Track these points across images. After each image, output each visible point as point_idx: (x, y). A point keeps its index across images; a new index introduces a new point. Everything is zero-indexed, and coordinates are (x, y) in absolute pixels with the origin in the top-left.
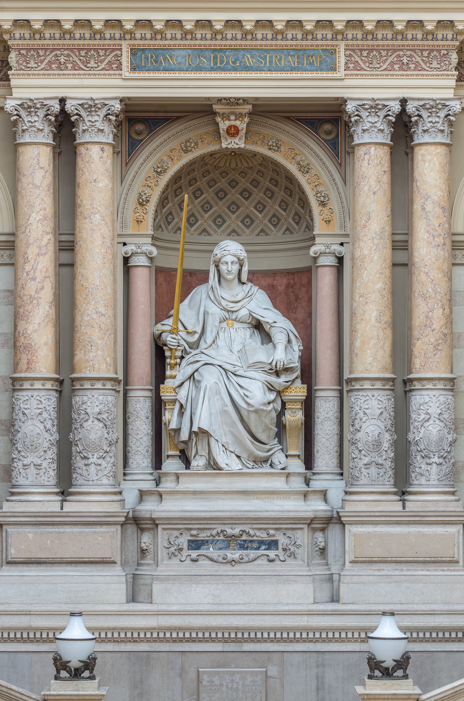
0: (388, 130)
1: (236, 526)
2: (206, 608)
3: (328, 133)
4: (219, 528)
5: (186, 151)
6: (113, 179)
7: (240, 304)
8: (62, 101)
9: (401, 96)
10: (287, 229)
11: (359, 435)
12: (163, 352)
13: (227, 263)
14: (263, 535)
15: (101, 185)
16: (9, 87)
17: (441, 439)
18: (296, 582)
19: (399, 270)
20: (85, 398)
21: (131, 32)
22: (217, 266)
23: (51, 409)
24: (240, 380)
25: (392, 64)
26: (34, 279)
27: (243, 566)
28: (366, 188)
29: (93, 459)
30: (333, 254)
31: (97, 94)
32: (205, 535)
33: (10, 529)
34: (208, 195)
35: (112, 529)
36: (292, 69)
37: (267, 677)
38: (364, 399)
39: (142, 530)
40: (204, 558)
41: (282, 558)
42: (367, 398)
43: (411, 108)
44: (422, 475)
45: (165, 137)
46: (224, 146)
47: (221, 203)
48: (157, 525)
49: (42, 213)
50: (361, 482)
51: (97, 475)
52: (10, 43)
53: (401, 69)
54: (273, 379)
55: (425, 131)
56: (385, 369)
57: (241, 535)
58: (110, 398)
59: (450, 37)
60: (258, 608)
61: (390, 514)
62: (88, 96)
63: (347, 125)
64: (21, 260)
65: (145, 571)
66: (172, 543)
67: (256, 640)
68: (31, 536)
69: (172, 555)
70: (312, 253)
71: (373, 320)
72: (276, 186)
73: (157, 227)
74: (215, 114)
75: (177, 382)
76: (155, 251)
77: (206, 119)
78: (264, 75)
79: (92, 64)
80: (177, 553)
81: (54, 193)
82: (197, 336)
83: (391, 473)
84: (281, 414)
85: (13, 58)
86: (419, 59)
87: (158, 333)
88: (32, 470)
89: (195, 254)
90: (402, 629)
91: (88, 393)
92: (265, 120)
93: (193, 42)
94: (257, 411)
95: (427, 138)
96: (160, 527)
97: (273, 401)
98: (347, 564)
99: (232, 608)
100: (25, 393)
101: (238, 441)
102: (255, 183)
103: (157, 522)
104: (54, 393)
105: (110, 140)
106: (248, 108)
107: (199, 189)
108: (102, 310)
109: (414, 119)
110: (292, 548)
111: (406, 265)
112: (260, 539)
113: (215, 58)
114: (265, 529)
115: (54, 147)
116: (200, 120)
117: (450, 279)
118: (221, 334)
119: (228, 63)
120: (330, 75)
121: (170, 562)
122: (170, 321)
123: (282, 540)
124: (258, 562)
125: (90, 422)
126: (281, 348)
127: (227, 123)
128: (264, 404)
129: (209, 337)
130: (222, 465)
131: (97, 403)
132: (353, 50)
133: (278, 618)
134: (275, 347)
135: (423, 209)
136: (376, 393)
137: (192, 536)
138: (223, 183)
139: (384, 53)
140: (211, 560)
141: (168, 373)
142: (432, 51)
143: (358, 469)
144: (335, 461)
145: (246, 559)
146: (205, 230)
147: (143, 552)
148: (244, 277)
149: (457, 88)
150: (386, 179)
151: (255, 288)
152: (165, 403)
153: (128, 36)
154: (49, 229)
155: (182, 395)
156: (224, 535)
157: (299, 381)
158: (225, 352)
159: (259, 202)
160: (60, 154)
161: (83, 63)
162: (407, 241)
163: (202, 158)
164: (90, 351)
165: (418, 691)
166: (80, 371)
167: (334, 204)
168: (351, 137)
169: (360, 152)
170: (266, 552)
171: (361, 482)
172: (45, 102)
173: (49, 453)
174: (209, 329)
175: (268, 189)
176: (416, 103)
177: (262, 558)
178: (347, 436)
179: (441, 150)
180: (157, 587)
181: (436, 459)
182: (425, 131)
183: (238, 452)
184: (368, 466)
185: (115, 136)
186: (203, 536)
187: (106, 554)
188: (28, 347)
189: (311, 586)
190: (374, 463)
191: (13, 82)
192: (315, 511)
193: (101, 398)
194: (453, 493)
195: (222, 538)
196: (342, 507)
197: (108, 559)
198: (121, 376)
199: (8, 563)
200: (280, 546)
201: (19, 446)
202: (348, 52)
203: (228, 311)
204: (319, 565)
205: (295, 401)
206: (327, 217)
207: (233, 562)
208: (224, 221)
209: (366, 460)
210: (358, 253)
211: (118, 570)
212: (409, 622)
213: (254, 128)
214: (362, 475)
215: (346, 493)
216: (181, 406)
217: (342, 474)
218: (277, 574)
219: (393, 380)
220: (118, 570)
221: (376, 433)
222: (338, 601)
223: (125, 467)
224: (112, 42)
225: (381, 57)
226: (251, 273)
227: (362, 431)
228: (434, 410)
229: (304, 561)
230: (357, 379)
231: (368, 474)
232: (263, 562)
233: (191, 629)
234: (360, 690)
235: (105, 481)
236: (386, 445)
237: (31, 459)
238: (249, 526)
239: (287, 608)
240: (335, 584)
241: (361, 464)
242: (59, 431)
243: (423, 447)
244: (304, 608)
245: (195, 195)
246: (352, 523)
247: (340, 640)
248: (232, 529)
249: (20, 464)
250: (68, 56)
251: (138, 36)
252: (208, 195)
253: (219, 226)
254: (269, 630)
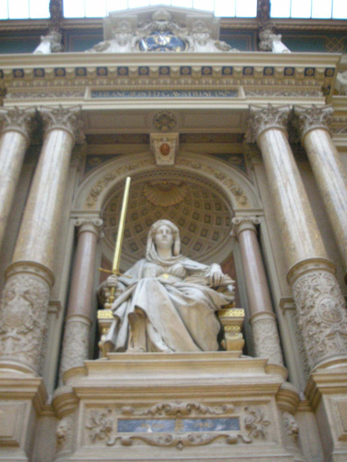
1: (182, 400)
4: (160, 403)
11: (313, 312)
13: (162, 232)
22: (154, 240)
29: (12, 333)
30: (251, 222)
32: (141, 413)
35: (20, 403)
38: (310, 279)
40: (139, 441)
41: (246, 439)
42: (314, 277)
50: (327, 355)
51: (13, 349)
57: (189, 411)
66: (98, 422)
69: (95, 439)
80: (103, 435)
91: (19, 276)
96: (82, 403)
103: (79, 395)
112: (214, 416)
114: (220, 404)
121: (92, 447)
125: (15, 299)
131: (27, 284)
137: (125, 413)
140: (150, 443)
143: (320, 342)
145: (198, 440)
147: (60, 439)
152: (102, 328)
156: (167, 412)
167: (246, 192)
171: (327, 355)
177: (220, 440)
184: (332, 337)
190: (337, 333)
193: (31, 281)
195: (164, 415)
197: (8, 439)
200: (242, 424)
207: (179, 444)
209: (328, 331)
214: (328, 348)
218: (243, 456)
227: (316, 306)
229: (276, 441)
231: (334, 344)
232: (221, 444)
235: (22, 358)
238: (199, 400)
241: (322, 337)
248: (177, 403)
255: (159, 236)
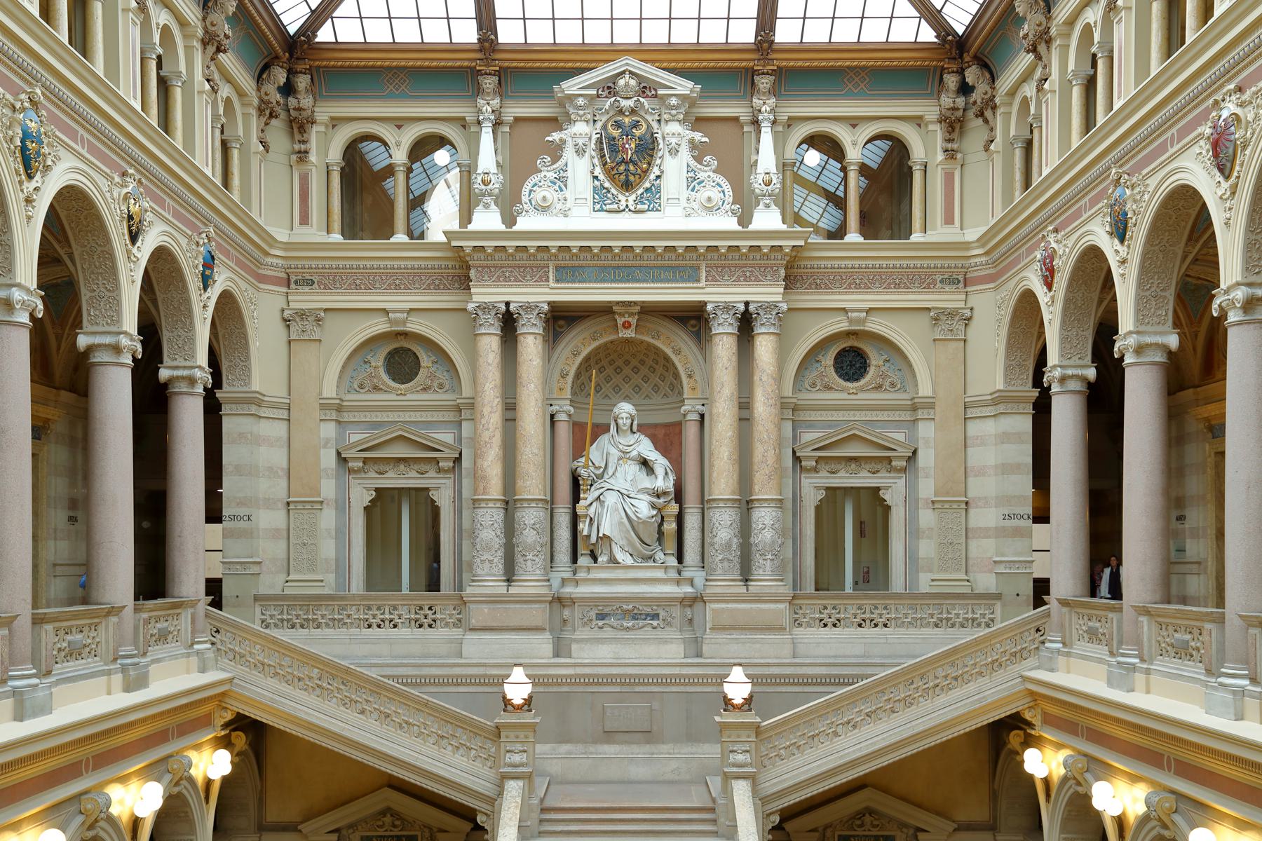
0: (736, 324)
2: (610, 661)
3: (693, 326)
5: (594, 340)
6: (543, 359)
7: (632, 447)
8: (507, 304)
9: (745, 300)
10: (665, 395)
12: (578, 481)
14: (649, 610)
15: (534, 363)
16: (471, 294)
17: (773, 542)
18: (672, 643)
19: (744, 423)
20: (524, 514)
21: (555, 256)
22: (616, 421)
23: (500, 521)
24: (632, 501)
25: (739, 277)
26: (488, 429)
27: (635, 632)
28: (720, 365)
29: (530, 557)
31: (531, 299)
33: (472, 606)
34: (610, 371)
36: (668, 281)
37: (651, 710)
39: (564, 606)
43: (752, 308)
44: (760, 568)
45: (579, 329)
46: (620, 335)
47: (619, 376)
48: (574, 603)
49: (493, 383)
50: (717, 573)
52: (470, 263)
53: (745, 280)
54: (655, 500)
55: (761, 325)
56: (733, 493)
58: (541, 514)
59: (779, 257)
60: (645, 661)
61: (738, 595)
62: (526, 300)
63: (707, 321)
64: (479, 416)
65: (566, 635)
67: (644, 684)
68: (486, 610)
69: (584, 625)
70: (682, 412)
71: (726, 458)
72: (657, 364)
73: (574, 393)
74: (614, 313)
75: (588, 502)
76: (572, 409)
77: (608, 317)
78: (648, 285)
79: (528, 278)
81: (502, 368)
82: (602, 470)
83: (738, 566)
84: (661, 525)
85: (472, 273)
86: (757, 273)
87: (574, 467)
88: (487, 564)
89: (599, 412)
90: (747, 676)
91: (526, 510)
92: (649, 317)
93: (599, 262)
94: (644, 522)
95: (763, 330)
97: (655, 515)
98: (708, 630)
99: (627, 661)
100: (481, 510)
101: (631, 543)
102: (642, 362)
104: (502, 510)
105: (541, 332)
106: (637, 309)
107: (603, 367)
108: (535, 451)
109: (754, 316)
110: (669, 619)
111: (749, 419)
113: (615, 273)
115: (502, 337)
116: (604, 318)
117: (780, 429)
118: (619, 468)
119: (623, 276)
120: (695, 285)
122: (583, 460)
123: (662, 614)
124: (646, 629)
126: (660, 478)
127: (623, 320)
128: (649, 518)
129: (610, 471)
130: (620, 561)
132: (712, 267)
133: (659, 668)
134: (656, 477)
135: (761, 380)
136: (726, 509)
138: (620, 363)
139: (733, 269)
140: (612, 627)
141: (582, 496)
142: (767, 267)
144: (699, 558)
146: (607, 396)
148: (635, 428)
149: (784, 294)
150: (734, 359)
151: (642, 437)
153: (553, 258)
154: (498, 395)
155: (592, 511)
157: (673, 501)
158: (622, 481)
159: (645, 376)
160: (505, 342)
161: (521, 276)
162: (749, 403)
163: (606, 344)
164: (527, 480)
165: (759, 720)
166: (521, 495)
167: (697, 376)
168: (710, 329)
169: (716, 339)
170: (651, 622)
171: (717, 573)
172: (496, 305)
173: (499, 552)
174: (610, 465)
175: (651, 367)
176: (755, 305)
178: (707, 540)
179: (772, 337)
180: (574, 647)
181: (770, 557)
182: (761, 325)
183: (630, 551)
185: (544, 329)
186: (606, 610)
187: (539, 623)
188: (484, 478)
189: (682, 646)
191: (473, 290)
192: (685, 593)
194: (782, 580)
195: (620, 611)
196: (704, 590)
198: (549, 499)
199: (471, 629)
200: (661, 617)
201: (478, 547)
202: (708, 269)
203: (624, 452)
204: (689, 631)
205: (671, 515)
206: (693, 386)
208: (620, 389)
210: (715, 411)
211: (547, 635)
212: (751, 671)
213: (641, 323)
215: (707, 580)
216: (591, 519)
217: (703, 567)
219: (739, 500)
220: (547, 635)
221: (728, 538)
222: (701, 656)
223: (551, 562)
224: (542, 262)
225: (731, 272)
226: (638, 425)
228: (768, 521)
230: (714, 500)
233: (598, 676)
234: (718, 719)
235: (538, 572)
236: (734, 547)
237: (486, 556)
239: (665, 661)
240: (699, 644)
242: (506, 537)
243: (760, 548)
244: (678, 661)
245: (600, 371)
246: (711, 601)
247: (703, 684)
249: (478, 560)
250: (511, 272)
251: (560, 257)
252: (610, 371)
253: (617, 393)
254: (653, 676)
255: (620, 422)
